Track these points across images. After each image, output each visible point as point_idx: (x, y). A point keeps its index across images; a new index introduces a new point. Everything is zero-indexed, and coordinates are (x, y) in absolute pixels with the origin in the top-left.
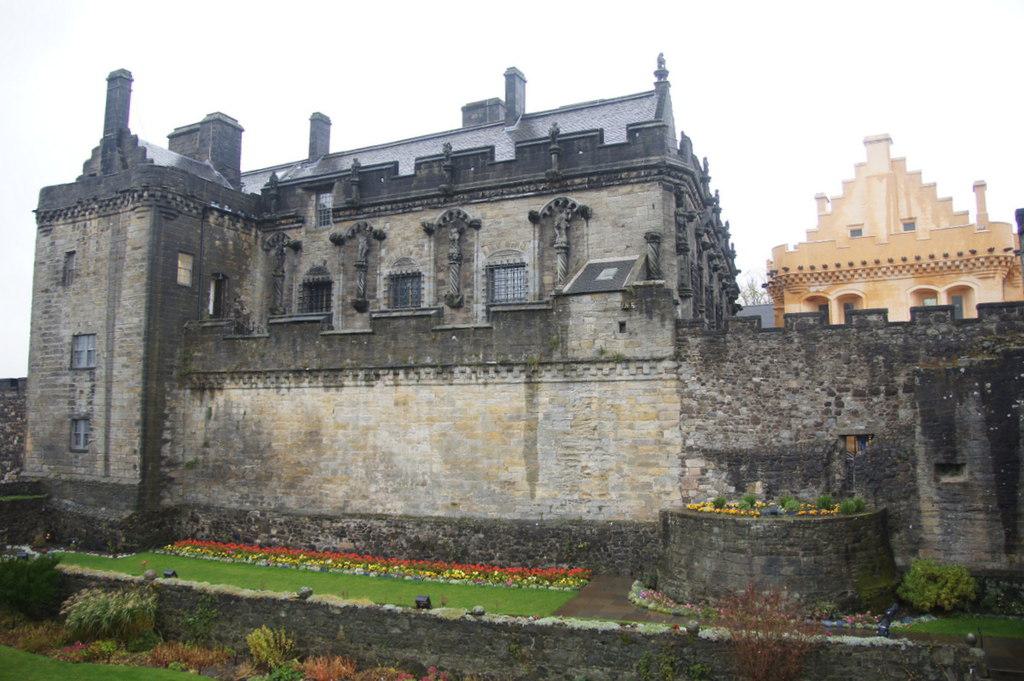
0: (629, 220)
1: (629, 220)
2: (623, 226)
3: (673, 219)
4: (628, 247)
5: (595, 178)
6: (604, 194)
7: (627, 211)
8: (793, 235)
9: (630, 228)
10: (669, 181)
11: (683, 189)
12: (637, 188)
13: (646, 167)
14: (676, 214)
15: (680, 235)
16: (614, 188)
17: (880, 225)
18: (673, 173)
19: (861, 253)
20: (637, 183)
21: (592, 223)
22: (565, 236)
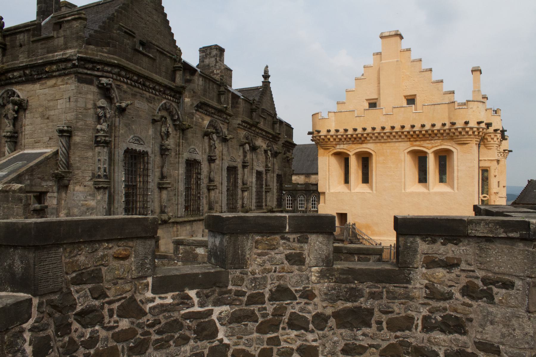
0: (52, 113)
1: (52, 113)
2: (48, 118)
3: (91, 111)
4: (50, 139)
5: (27, 72)
6: (37, 86)
7: (51, 104)
8: (326, 106)
9: (52, 121)
10: (86, 74)
11: (104, 80)
12: (60, 80)
13: (61, 61)
14: (95, 107)
15: (99, 127)
16: (44, 82)
17: (391, 99)
18: (91, 66)
19: (375, 120)
20: (60, 76)
21: (28, 115)
22: (12, 126)
